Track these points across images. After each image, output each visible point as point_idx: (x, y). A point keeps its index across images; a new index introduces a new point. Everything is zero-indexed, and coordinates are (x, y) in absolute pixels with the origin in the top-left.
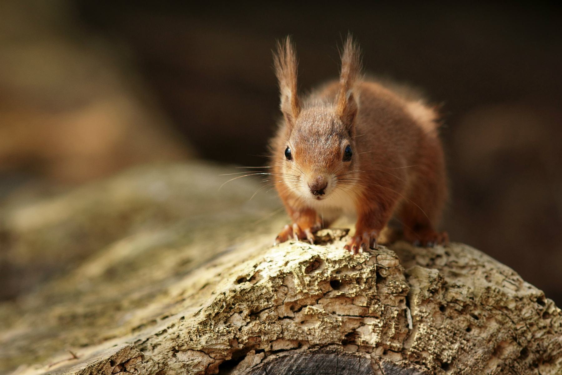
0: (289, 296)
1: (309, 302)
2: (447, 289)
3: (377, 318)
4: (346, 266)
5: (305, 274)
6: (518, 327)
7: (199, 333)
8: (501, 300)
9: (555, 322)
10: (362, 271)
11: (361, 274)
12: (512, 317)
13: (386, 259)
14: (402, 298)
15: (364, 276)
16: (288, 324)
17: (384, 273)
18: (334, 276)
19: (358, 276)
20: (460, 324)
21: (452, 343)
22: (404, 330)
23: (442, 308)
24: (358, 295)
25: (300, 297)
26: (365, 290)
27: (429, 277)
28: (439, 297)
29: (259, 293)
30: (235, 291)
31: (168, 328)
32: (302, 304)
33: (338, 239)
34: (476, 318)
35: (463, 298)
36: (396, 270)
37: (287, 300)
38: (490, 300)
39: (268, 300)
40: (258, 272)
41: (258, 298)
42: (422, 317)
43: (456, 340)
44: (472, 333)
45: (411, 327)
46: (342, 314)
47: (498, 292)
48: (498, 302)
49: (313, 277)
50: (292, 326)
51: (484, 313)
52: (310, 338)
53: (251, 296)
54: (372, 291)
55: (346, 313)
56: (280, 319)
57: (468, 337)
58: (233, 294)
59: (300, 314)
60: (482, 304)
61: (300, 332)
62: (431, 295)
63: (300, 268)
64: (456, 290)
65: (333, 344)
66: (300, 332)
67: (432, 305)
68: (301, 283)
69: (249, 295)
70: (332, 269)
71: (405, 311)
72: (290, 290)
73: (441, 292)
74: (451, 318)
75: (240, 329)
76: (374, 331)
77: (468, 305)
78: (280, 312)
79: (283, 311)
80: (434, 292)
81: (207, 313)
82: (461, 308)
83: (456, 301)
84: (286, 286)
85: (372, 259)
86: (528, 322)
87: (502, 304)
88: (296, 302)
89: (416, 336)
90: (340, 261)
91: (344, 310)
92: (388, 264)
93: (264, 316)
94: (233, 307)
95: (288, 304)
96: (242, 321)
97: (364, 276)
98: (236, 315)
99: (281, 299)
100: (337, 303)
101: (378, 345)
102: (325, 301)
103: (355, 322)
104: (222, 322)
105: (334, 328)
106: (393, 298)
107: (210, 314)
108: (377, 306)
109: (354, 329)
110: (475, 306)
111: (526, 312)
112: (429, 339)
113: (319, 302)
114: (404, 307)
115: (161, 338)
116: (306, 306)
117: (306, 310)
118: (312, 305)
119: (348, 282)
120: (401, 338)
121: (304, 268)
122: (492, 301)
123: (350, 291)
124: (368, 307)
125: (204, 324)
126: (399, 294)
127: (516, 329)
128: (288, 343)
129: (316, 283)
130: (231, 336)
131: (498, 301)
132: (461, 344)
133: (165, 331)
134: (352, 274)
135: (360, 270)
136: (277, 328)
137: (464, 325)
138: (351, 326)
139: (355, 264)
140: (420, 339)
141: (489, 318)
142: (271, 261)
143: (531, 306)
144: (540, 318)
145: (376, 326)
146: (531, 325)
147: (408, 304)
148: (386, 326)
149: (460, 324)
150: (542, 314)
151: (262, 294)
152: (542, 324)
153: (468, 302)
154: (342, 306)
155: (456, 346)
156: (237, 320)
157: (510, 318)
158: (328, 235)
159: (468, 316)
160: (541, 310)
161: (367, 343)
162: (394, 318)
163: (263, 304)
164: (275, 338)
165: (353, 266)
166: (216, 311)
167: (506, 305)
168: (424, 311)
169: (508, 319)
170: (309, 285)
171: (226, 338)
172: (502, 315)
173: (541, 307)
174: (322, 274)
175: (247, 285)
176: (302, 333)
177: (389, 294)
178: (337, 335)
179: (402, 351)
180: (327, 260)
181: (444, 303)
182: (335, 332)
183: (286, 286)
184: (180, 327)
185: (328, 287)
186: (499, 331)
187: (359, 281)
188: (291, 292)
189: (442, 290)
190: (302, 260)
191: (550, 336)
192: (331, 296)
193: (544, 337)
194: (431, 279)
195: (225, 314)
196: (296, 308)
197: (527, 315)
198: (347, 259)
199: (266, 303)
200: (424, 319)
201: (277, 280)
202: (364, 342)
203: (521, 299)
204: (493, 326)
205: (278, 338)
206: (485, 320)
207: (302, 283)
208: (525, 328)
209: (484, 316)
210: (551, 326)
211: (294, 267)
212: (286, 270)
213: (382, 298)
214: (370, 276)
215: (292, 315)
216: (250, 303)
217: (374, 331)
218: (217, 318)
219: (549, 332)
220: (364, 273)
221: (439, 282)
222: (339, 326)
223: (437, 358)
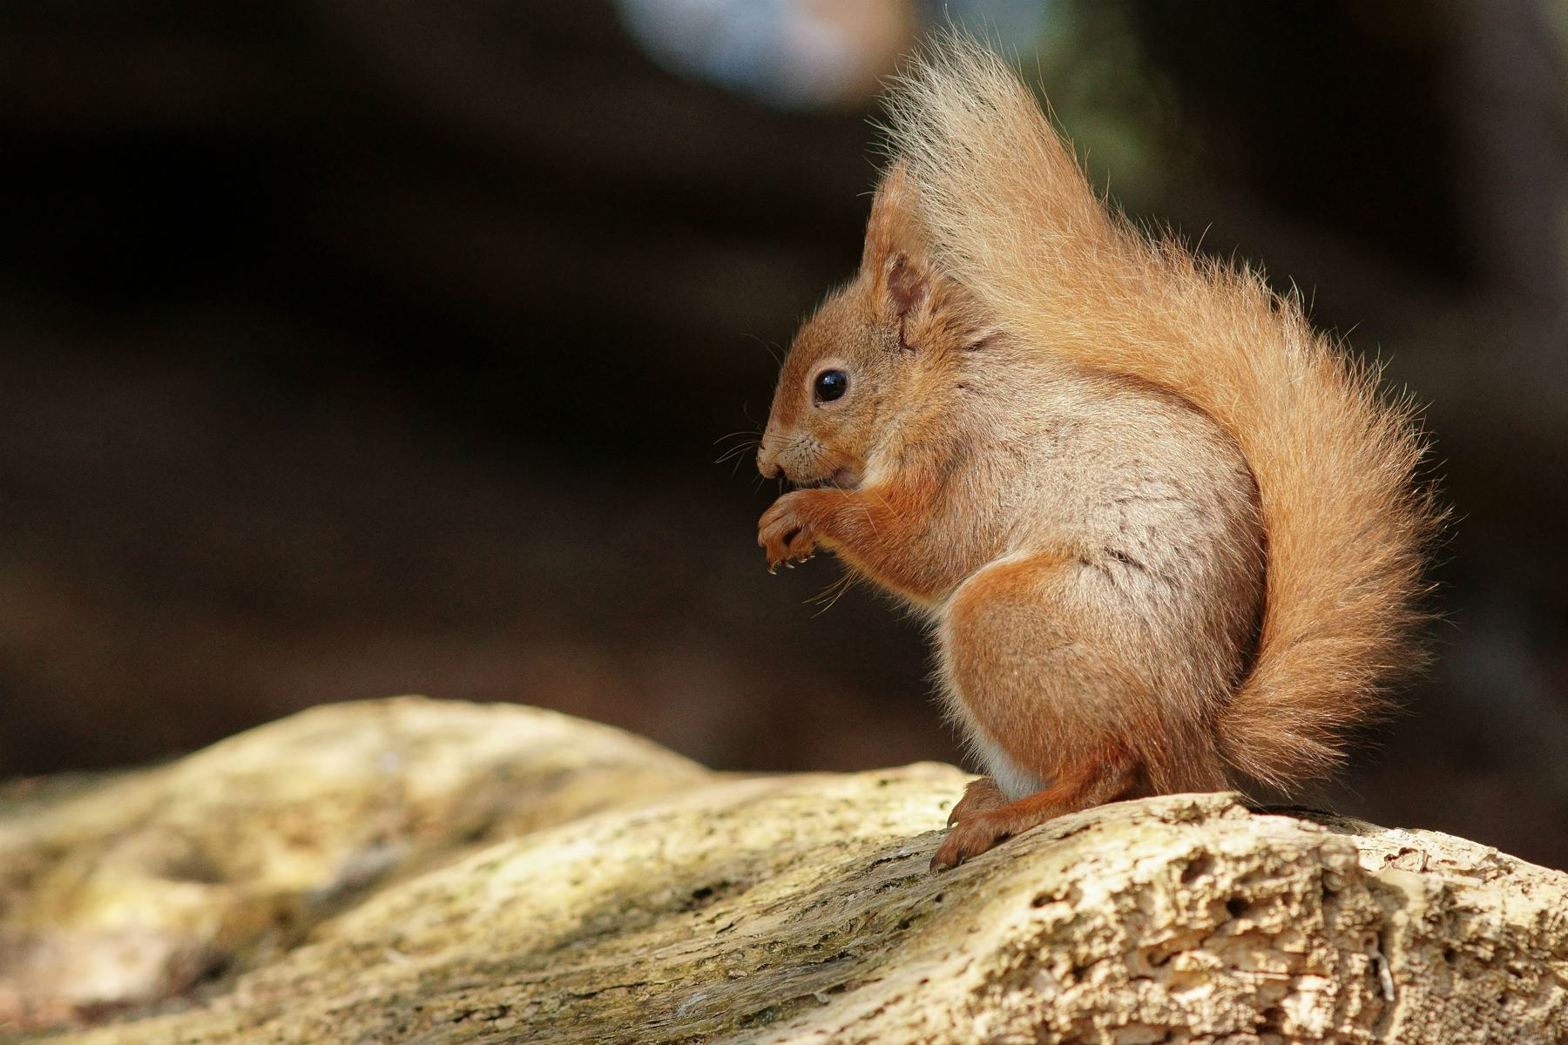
3: (1324, 976)
4: (1260, 868)
7: (971, 1011)
11: (1291, 884)
14: (1372, 935)
15: (1297, 888)
16: (1148, 991)
17: (1336, 882)
19: (1285, 889)
21: (1474, 1028)
22: (1377, 1003)
23: (1450, 954)
24: (1288, 930)
25: (1169, 934)
26: (1298, 919)
27: (1427, 891)
30: (1041, 922)
31: (887, 1004)
32: (1174, 949)
33: (1215, 815)
34: (1519, 974)
37: (1147, 941)
39: (1108, 940)
40: (1073, 883)
41: (1089, 938)
42: (1414, 974)
43: (1481, 1022)
44: (1508, 1008)
45: (1390, 997)
50: (1154, 992)
52: (1192, 1020)
56: (1131, 979)
57: (1505, 1016)
58: (1037, 929)
59: (1167, 969)
62: (1430, 927)
65: (1237, 1031)
76: (1318, 1004)
77: (1504, 948)
81: (987, 969)
88: (1159, 946)
89: (1400, 1013)
90: (1249, 858)
93: (1099, 973)
95: (1142, 950)
97: (1297, 888)
98: (1044, 973)
101: (1328, 1033)
102: (1221, 942)
105: (1240, 999)
108: (1323, 951)
109: (1276, 1001)
110: (1517, 949)
112: (1429, 1021)
113: (1207, 943)
115: (880, 1022)
116: (1178, 953)
117: (1181, 962)
118: (1192, 949)
119: (1266, 903)
120: (1370, 1020)
121: (1177, 873)
123: (1270, 921)
124: (1305, 955)
125: (981, 992)
126: (1367, 926)
128: (1147, 1031)
129: (1202, 904)
132: (1492, 1029)
133: (880, 1011)
134: (1270, 884)
136: (1126, 999)
137: (1492, 993)
139: (1278, 862)
140: (1409, 1020)
142: (1095, 861)
145: (1323, 993)
148: (1343, 994)
153: (1503, 943)
158: (1194, 806)
159: (1503, 972)
161: (1306, 1030)
162: (1356, 977)
163: (1098, 948)
164: (1123, 1020)
168: (1416, 961)
170: (1188, 908)
171: (1025, 1021)
174: (1213, 885)
175: (1062, 911)
178: (1246, 1013)
180: (1223, 856)
181: (1456, 944)
182: (1242, 1007)
184: (919, 1002)
185: (1224, 913)
187: (1287, 898)
190: (1173, 855)
194: (1431, 895)
196: (1160, 958)
202: (1299, 1027)
205: (1130, 1021)
211: (1156, 870)
212: (1140, 876)
214: (1309, 887)
215: (1150, 972)
217: (1318, 1004)
222: (1249, 995)
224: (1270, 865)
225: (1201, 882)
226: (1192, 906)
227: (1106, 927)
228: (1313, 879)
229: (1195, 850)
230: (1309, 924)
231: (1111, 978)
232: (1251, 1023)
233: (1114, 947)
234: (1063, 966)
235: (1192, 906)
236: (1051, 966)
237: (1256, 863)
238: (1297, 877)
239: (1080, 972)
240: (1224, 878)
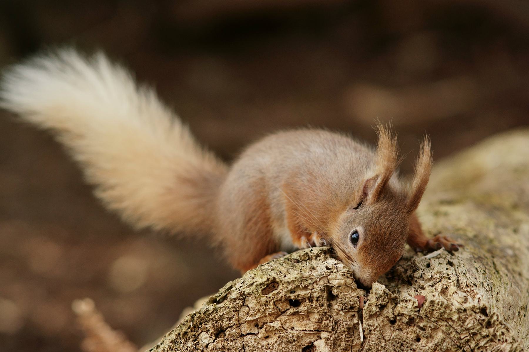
0: (250, 315)
1: (268, 319)
2: (396, 304)
4: (298, 287)
5: (261, 295)
6: (462, 337)
8: (444, 312)
9: (497, 331)
10: (313, 290)
12: (456, 328)
13: (336, 278)
14: (353, 313)
15: (315, 295)
17: (335, 292)
18: (288, 295)
20: (409, 335)
25: (259, 315)
26: (316, 308)
28: (389, 312)
29: (221, 314)
35: (408, 311)
36: (348, 288)
38: (435, 312)
39: (230, 319)
46: (299, 329)
47: (441, 305)
48: (442, 314)
49: (270, 298)
51: (429, 325)
53: (215, 317)
54: (323, 308)
55: (303, 328)
60: (426, 316)
61: (259, 346)
62: (378, 310)
64: (404, 304)
66: (259, 346)
67: (381, 318)
68: (259, 303)
69: (213, 316)
70: (286, 290)
71: (358, 324)
72: (251, 310)
73: (390, 306)
74: (401, 330)
75: (207, 346)
78: (242, 329)
79: (245, 328)
80: (382, 307)
82: (407, 320)
83: (403, 315)
84: (248, 306)
85: (323, 279)
86: (472, 331)
87: (446, 316)
91: (301, 326)
92: (338, 283)
94: (200, 326)
95: (249, 322)
96: (208, 338)
97: (315, 295)
99: (243, 318)
100: (294, 320)
102: (283, 318)
103: (312, 336)
104: (191, 340)
106: (343, 314)
107: (179, 334)
109: (310, 343)
111: (469, 323)
114: (356, 321)
121: (260, 289)
122: (436, 314)
127: (460, 339)
131: (441, 313)
135: (311, 290)
137: (412, 336)
138: (308, 340)
141: (436, 329)
143: (473, 317)
144: (483, 327)
146: (475, 334)
147: (361, 318)
149: (409, 335)
150: (484, 324)
151: (223, 314)
152: (484, 334)
153: (413, 316)
154: (299, 322)
157: (453, 328)
160: (484, 320)
165: (305, 286)
166: (184, 331)
167: (450, 317)
169: (452, 330)
172: (446, 326)
173: (483, 317)
174: (278, 293)
176: (261, 348)
177: (340, 310)
180: (281, 281)
182: (291, 346)
183: (248, 306)
186: (443, 340)
187: (311, 299)
188: (252, 311)
189: (392, 304)
191: (493, 343)
192: (288, 314)
193: (487, 345)
194: (378, 296)
195: (193, 333)
197: (469, 326)
198: (299, 280)
199: (228, 322)
200: (372, 332)
201: (238, 301)
203: (465, 310)
204: (440, 335)
206: (430, 331)
208: (468, 338)
209: (430, 327)
210: (495, 335)
212: (247, 291)
216: (214, 323)
218: (186, 337)
219: (492, 340)
220: (315, 292)
221: (385, 298)
229: (268, 280)
235: (266, 304)
237: (296, 284)
238: (315, 290)
240: (282, 290)
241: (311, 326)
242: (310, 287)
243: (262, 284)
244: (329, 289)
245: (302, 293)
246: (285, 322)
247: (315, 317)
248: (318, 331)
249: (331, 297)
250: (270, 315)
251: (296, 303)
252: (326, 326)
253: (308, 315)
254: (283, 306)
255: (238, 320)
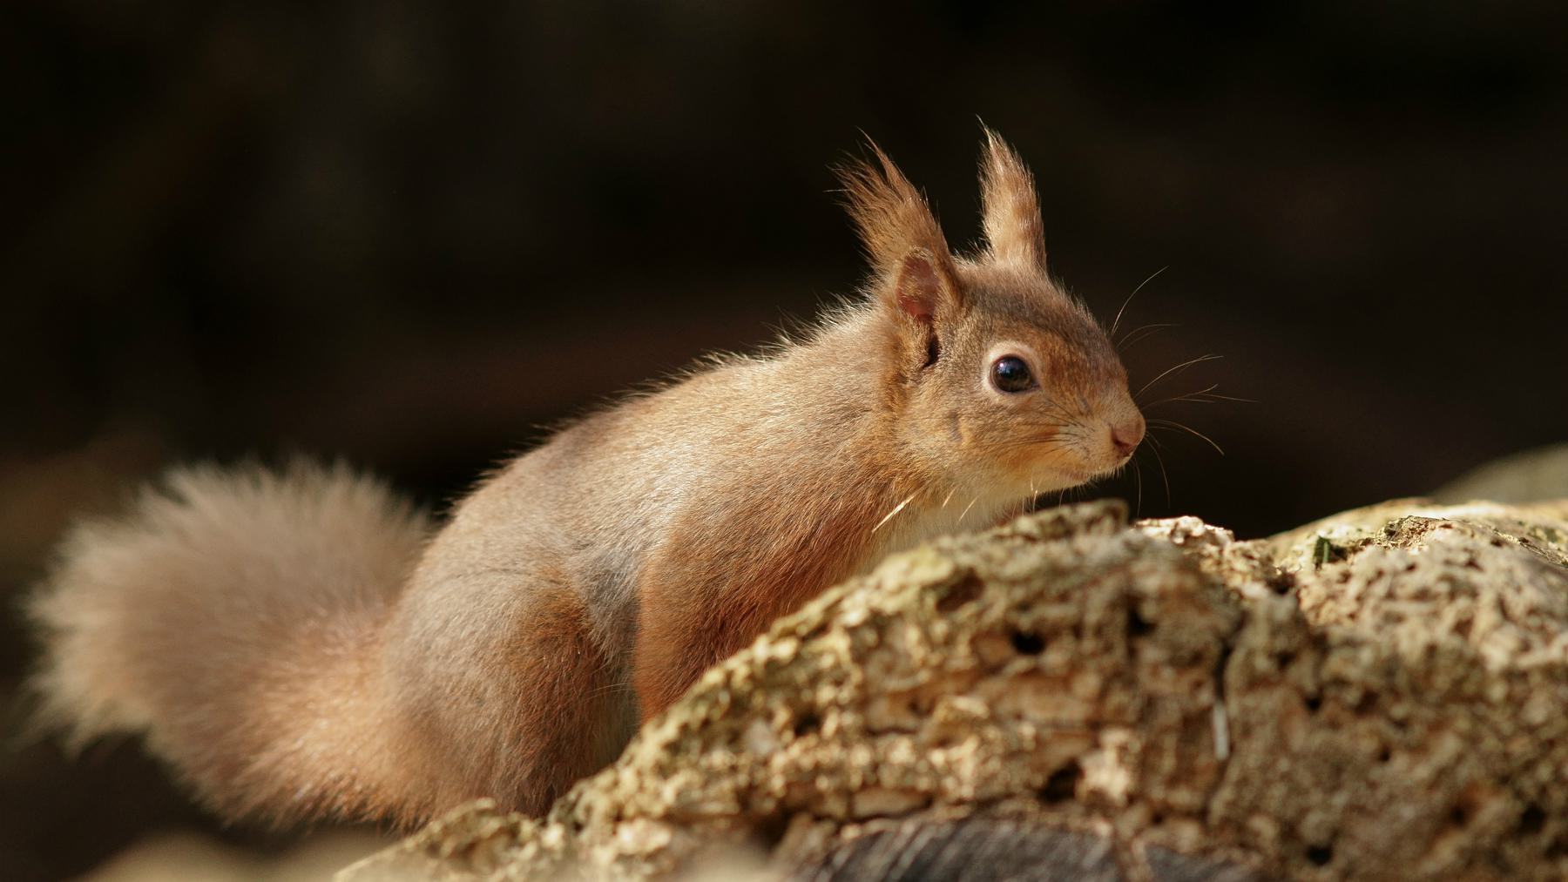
13: (1152, 571)
17: (1149, 611)
37: (894, 684)
41: (815, 680)
52: (949, 783)
63: (921, 599)
65: (1009, 796)
83: (1341, 682)
90: (1026, 580)
95: (895, 696)
97: (1092, 617)
102: (994, 686)
114: (1205, 697)
121: (931, 600)
130: (742, 779)
136: (861, 756)
147: (1221, 692)
155: (1340, 799)
156: (760, 737)
179: (1200, 815)
187: (1077, 630)
196: (918, 704)
207: (927, 638)
213: (1144, 676)
223: (1289, 831)
224: (1059, 585)
225: (967, 612)
226: (949, 641)
227: (837, 665)
228: (1112, 606)
230: (1107, 661)
231: (840, 731)
232: (1028, 786)
233: (846, 694)
234: (782, 716)
235: (949, 641)
236: (769, 716)
237: (1037, 585)
239: (807, 722)
240: (997, 604)
241: (1074, 710)
242: (1077, 595)
243: (935, 586)
244: (1130, 603)
245: (1053, 612)
246: (1000, 697)
247: (1088, 683)
248: (1094, 728)
249: (1138, 627)
250: (958, 674)
251: (1030, 643)
252: (1120, 711)
253: (1064, 681)
254: (997, 650)
255: (862, 687)
